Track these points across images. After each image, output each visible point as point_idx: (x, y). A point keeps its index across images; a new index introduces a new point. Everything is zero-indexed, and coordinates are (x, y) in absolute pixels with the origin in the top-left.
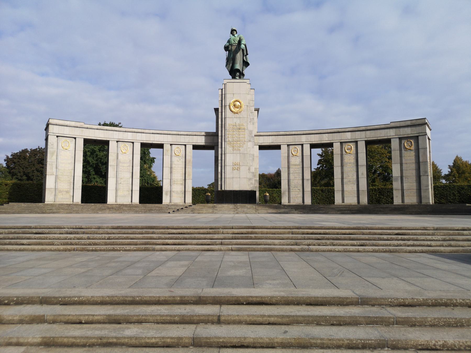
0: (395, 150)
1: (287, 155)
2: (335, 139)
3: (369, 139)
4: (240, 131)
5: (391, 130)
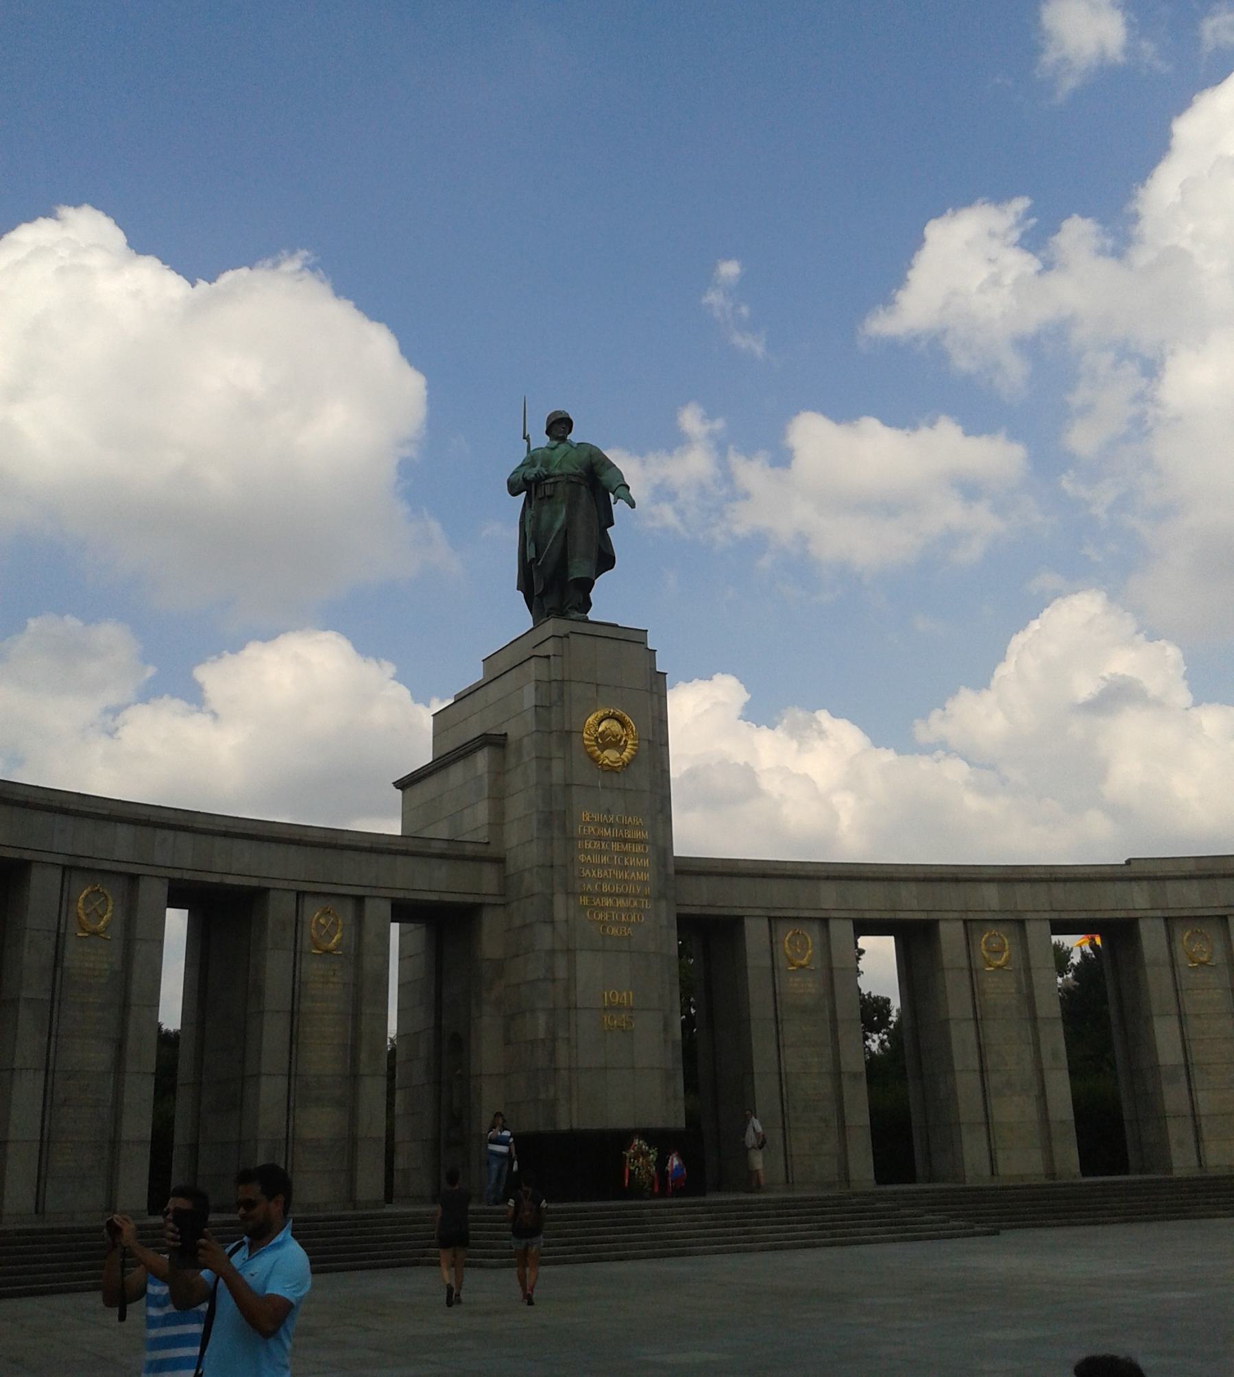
1: (768, 963)
2: (947, 907)
3: (1065, 916)
4: (628, 846)
5: (1135, 886)
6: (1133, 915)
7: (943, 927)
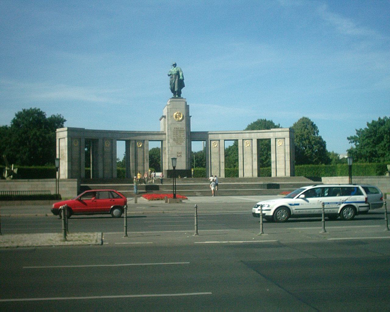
0: (273, 145)
2: (240, 137)
3: (259, 138)
6: (270, 138)
7: (239, 140)
